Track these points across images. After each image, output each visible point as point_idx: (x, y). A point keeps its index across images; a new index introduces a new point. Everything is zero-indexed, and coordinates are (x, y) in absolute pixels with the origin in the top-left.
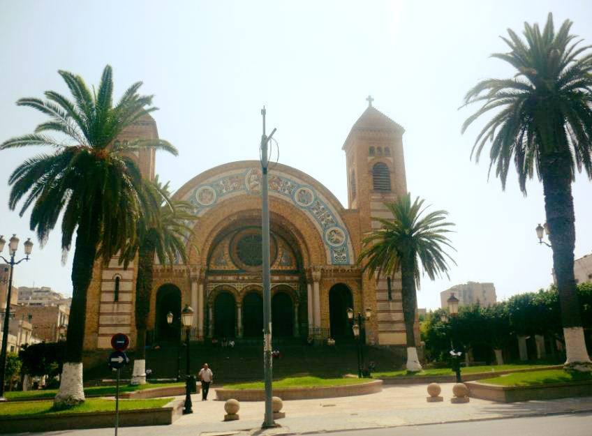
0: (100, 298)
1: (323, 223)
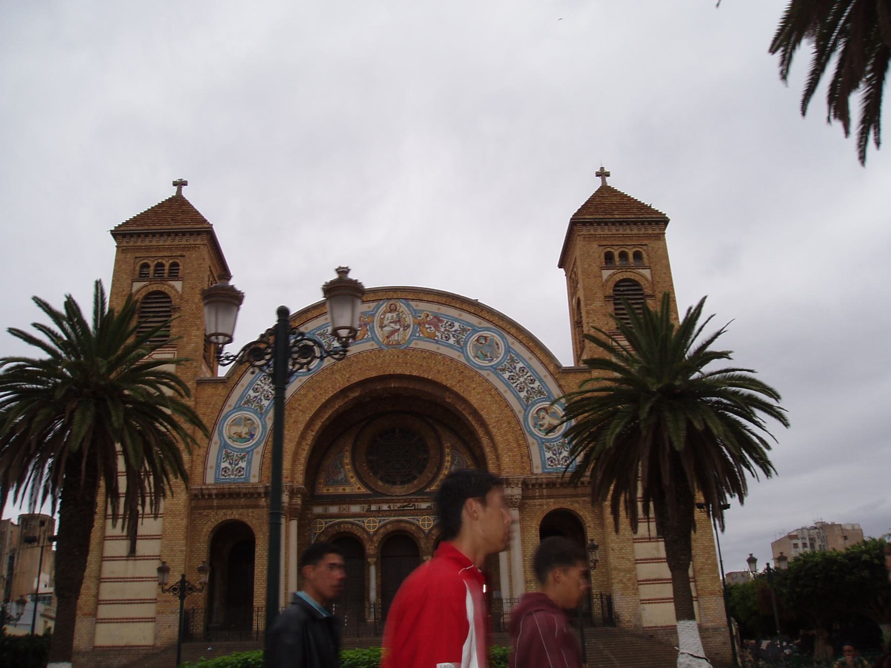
1: (523, 394)
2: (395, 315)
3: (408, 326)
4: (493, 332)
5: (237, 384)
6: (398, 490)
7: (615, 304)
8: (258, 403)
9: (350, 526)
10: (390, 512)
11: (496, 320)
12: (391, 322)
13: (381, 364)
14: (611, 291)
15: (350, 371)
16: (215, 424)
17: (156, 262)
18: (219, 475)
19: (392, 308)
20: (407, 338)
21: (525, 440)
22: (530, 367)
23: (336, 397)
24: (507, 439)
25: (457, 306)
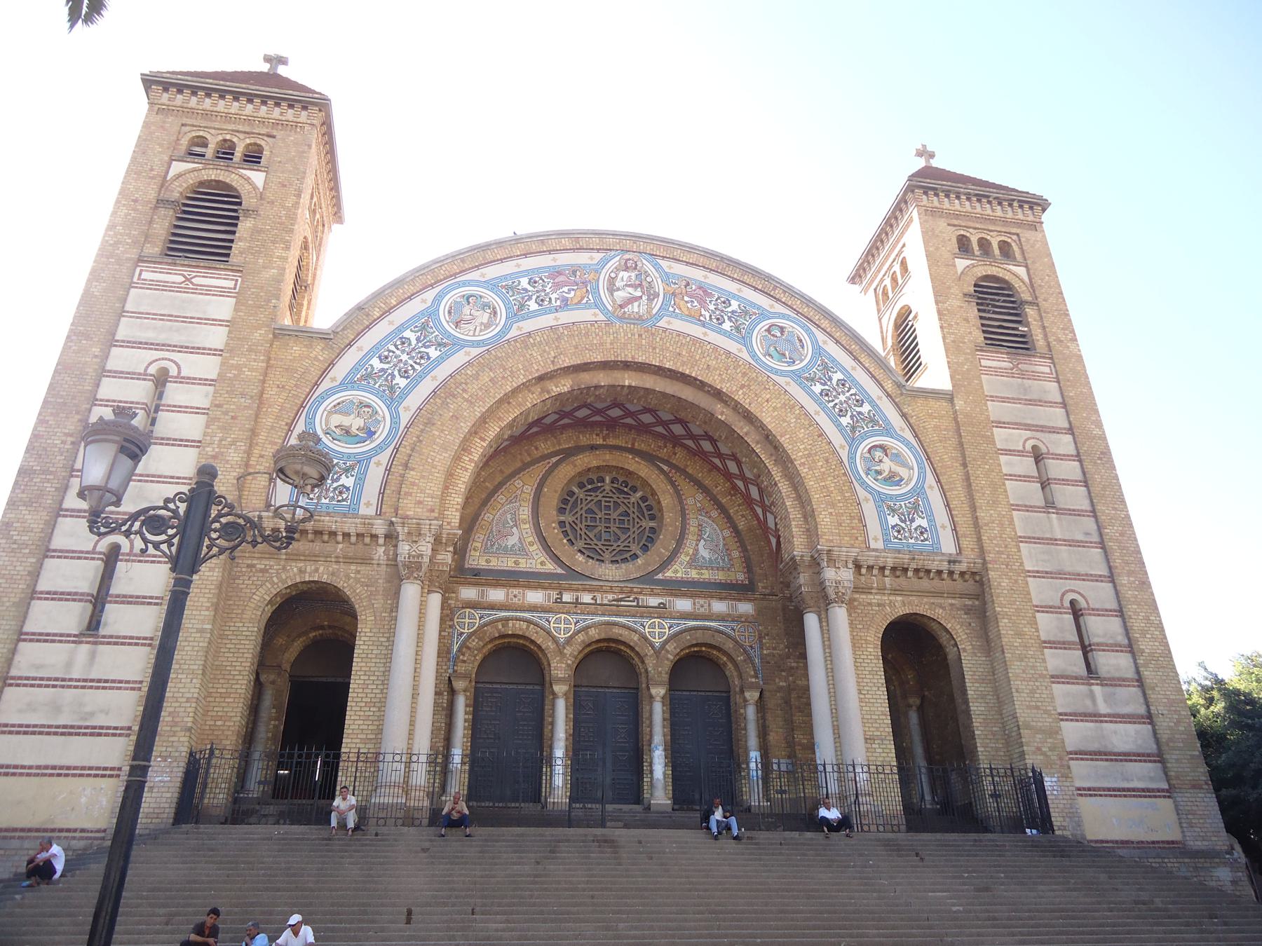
0: (24, 617)
2: (633, 275)
4: (793, 322)
5: (350, 345)
6: (609, 572)
7: (979, 310)
8: (386, 380)
9: (524, 625)
10: (595, 608)
11: (797, 304)
12: (626, 285)
13: (611, 344)
14: (972, 289)
15: (557, 347)
16: (302, 406)
17: (220, 138)
20: (654, 311)
22: (856, 383)
23: (526, 386)
25: (735, 276)
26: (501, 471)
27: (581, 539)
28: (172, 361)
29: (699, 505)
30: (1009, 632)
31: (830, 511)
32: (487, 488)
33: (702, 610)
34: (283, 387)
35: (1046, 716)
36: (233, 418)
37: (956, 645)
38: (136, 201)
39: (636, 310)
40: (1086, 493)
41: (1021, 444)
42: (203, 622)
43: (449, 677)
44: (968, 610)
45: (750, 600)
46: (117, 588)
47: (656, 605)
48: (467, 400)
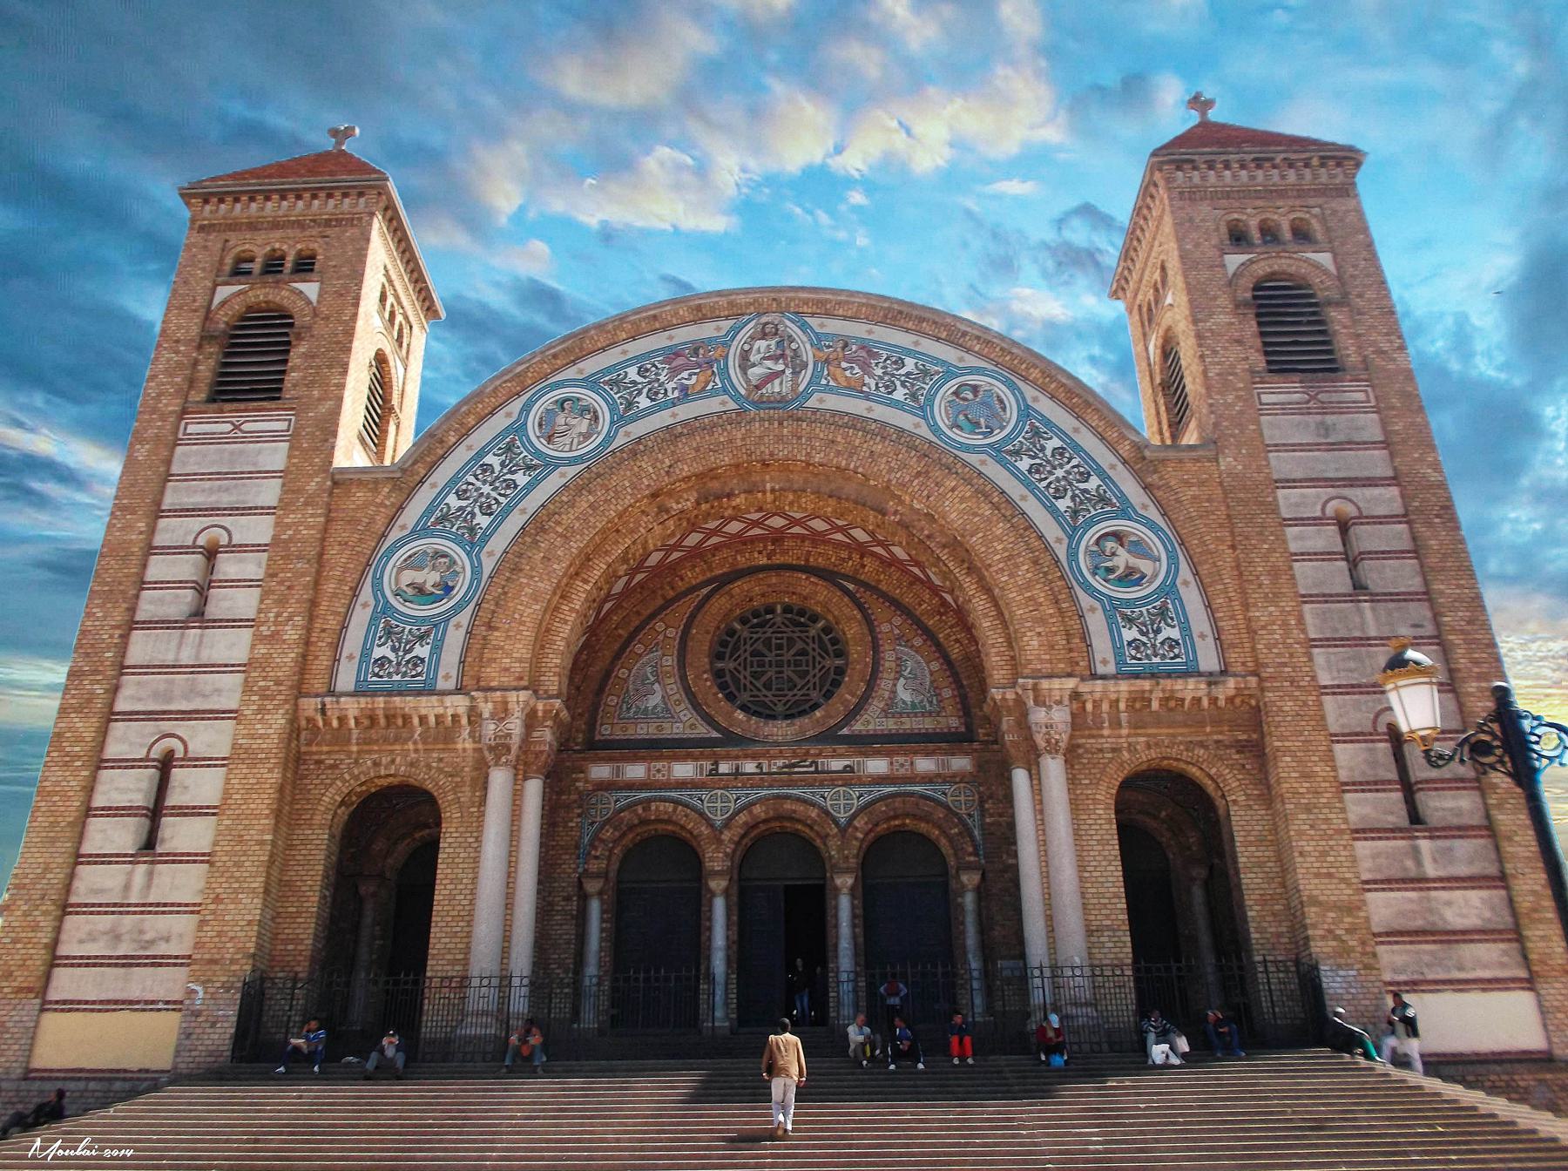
1: (1063, 504)
2: (773, 343)
3: (805, 366)
4: (993, 377)
5: (422, 482)
6: (780, 730)
7: (1260, 324)
9: (670, 807)
12: (764, 358)
14: (1248, 295)
16: (368, 565)
18: (366, 675)
19: (767, 331)
20: (801, 388)
21: (1073, 599)
22: (1077, 448)
24: (1031, 599)
26: (638, 613)
27: (745, 690)
28: (222, 527)
29: (897, 631)
30: (1293, 775)
31: (1038, 630)
32: (620, 636)
33: (902, 771)
34: (346, 544)
35: (1343, 886)
36: (289, 588)
37: (1223, 796)
38: (177, 341)
39: (777, 389)
40: (1418, 568)
41: (1319, 507)
42: (262, 832)
43: (579, 878)
44: (1241, 747)
45: (967, 754)
46: (173, 799)
47: (840, 768)
48: (561, 535)
